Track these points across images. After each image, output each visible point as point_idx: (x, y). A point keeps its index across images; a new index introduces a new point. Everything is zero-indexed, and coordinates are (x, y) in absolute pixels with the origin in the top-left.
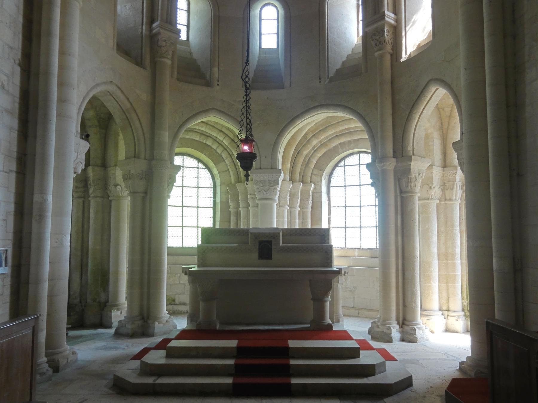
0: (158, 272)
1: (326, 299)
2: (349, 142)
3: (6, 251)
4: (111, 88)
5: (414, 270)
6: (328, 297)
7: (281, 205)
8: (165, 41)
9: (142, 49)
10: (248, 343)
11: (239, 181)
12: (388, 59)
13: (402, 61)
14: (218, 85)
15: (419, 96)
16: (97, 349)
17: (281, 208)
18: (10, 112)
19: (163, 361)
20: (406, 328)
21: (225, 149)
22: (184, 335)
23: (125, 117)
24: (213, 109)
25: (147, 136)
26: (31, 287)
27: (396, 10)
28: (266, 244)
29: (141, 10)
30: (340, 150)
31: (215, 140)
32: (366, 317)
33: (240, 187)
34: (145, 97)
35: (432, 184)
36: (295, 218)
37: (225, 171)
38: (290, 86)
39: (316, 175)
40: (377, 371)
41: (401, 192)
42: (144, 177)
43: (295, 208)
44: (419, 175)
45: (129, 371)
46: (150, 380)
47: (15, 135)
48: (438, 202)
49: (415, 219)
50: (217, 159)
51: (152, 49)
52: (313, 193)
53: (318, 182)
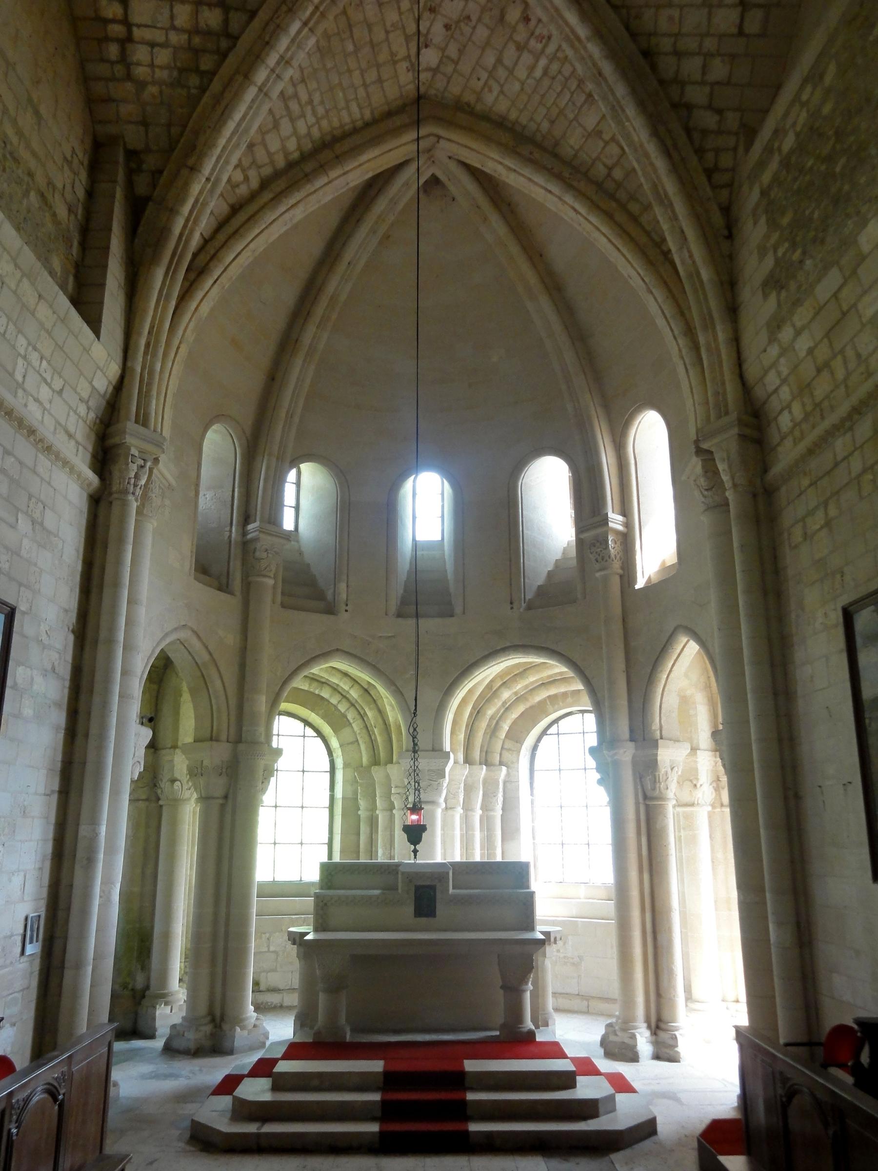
0: (243, 937)
1: (524, 987)
2: (565, 695)
3: (39, 916)
4: (182, 635)
5: (670, 930)
6: (527, 983)
8: (266, 550)
9: (229, 564)
10: (401, 1066)
11: (375, 761)
12: (616, 582)
13: (637, 587)
14: (346, 611)
15: (665, 646)
16: (144, 1077)
17: (450, 812)
18: (58, 705)
19: (267, 1097)
20: (662, 1035)
21: (353, 705)
22: (294, 1051)
23: (199, 674)
24: (337, 650)
25: (233, 702)
26: (68, 974)
27: (625, 510)
28: (426, 893)
29: (230, 503)
30: (550, 708)
31: (335, 689)
32: (601, 1014)
33: (377, 773)
34: (231, 639)
35: (697, 779)
36: (473, 829)
37: (352, 743)
38: (464, 613)
40: (601, 1110)
41: (645, 797)
42: (224, 770)
43: (472, 810)
44: (672, 769)
45: (216, 1114)
46: (251, 1128)
47: (61, 735)
48: (710, 808)
49: (669, 844)
50: (338, 722)
52: (505, 783)
53: (513, 763)
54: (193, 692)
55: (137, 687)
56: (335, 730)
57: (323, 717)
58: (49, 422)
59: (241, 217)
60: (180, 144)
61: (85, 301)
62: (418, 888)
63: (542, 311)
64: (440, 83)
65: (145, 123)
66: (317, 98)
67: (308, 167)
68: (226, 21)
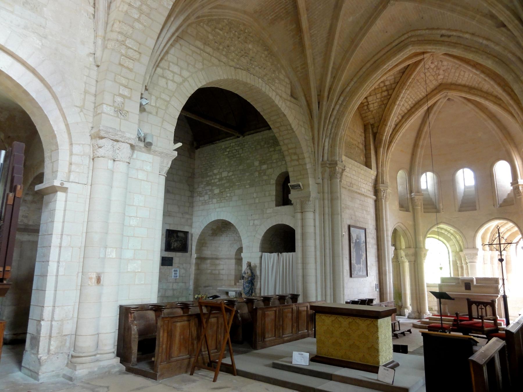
0: (423, 294)
4: (399, 224)
25: (414, 238)
26: (385, 295)
33: (461, 253)
34: (411, 223)
50: (448, 239)
51: (412, 203)
54: (403, 237)
55: (390, 239)
56: (448, 242)
57: (444, 238)
58: (366, 191)
59: (398, 127)
60: (382, 120)
61: (368, 165)
62: (465, 283)
63: (490, 125)
64: (445, 81)
65: (374, 118)
66: (412, 96)
67: (413, 110)
68: (388, 93)
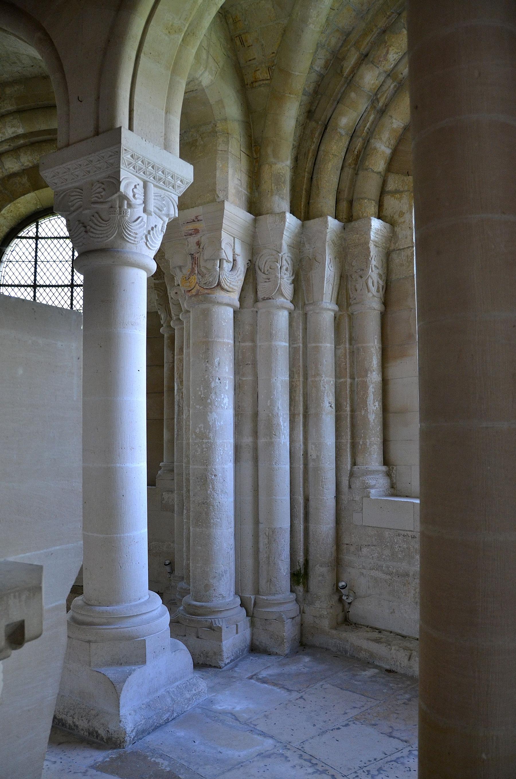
7: (260, 295)
39: (397, 192)
